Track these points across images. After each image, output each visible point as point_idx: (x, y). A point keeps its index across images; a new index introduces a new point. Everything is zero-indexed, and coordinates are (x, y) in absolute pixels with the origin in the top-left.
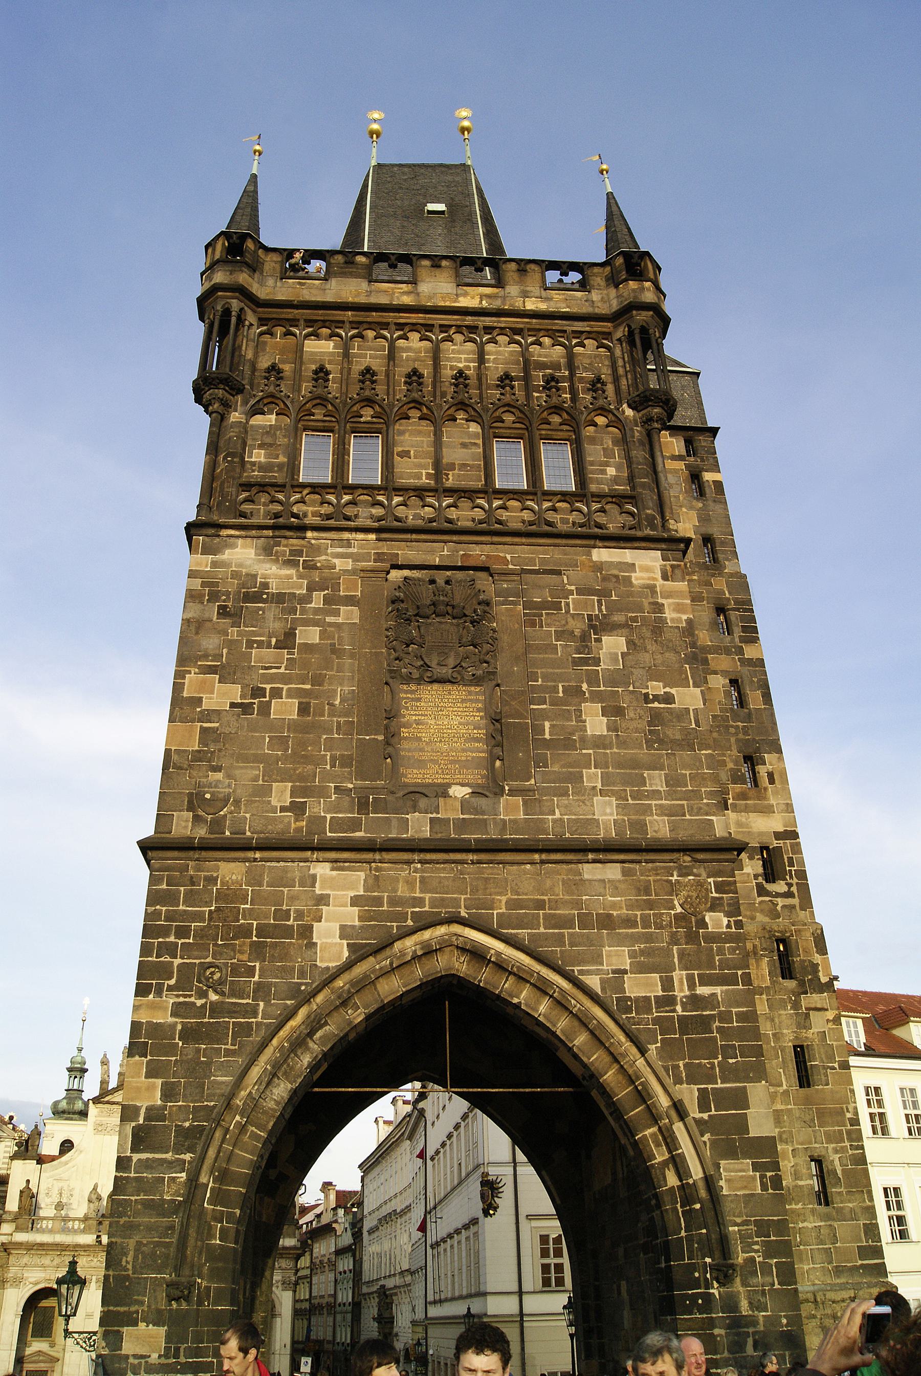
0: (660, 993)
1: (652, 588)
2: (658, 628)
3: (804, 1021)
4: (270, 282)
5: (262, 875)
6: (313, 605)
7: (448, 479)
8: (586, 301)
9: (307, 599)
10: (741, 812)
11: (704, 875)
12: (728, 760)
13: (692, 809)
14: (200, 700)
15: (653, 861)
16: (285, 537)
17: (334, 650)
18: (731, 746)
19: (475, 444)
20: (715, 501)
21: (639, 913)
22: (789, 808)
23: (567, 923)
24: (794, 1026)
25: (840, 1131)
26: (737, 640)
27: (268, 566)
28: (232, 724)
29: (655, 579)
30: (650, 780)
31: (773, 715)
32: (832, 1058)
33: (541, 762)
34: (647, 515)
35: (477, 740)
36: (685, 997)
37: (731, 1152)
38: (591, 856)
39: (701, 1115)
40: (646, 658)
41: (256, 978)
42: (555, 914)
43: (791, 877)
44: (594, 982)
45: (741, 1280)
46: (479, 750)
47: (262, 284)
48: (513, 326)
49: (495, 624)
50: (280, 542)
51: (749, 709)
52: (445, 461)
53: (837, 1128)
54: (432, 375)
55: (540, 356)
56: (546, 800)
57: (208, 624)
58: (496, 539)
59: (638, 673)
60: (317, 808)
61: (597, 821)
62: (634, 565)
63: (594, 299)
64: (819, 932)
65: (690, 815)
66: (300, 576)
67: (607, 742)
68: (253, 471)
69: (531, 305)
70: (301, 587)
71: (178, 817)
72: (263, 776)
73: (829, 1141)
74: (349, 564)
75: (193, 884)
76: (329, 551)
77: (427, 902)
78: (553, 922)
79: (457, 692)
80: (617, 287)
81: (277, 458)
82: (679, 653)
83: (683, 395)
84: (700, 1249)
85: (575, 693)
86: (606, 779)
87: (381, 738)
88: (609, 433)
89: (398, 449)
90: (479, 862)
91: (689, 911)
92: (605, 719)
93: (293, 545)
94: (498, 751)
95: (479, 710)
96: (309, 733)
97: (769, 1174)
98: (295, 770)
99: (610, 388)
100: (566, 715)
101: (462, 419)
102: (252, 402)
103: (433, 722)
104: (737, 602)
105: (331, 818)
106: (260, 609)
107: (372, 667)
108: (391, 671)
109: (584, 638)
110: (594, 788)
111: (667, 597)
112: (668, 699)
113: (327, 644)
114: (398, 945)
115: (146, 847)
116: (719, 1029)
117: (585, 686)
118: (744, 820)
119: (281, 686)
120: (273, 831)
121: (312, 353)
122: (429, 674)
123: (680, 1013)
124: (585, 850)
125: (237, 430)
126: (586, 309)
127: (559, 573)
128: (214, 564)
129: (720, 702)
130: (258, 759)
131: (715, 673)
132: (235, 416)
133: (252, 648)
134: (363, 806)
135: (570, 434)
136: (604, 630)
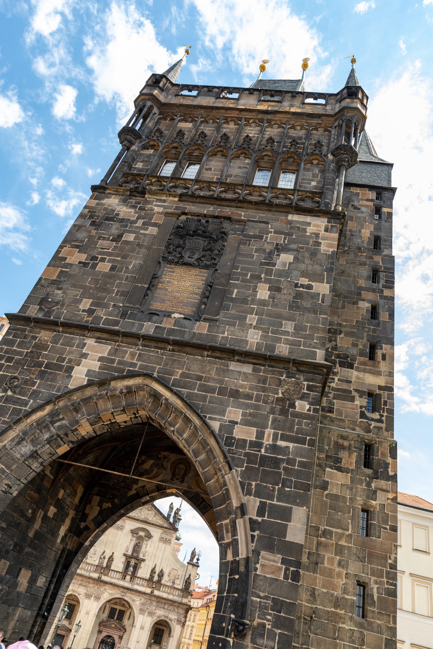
0: (254, 439)
1: (317, 235)
2: (314, 254)
3: (373, 495)
6: (136, 225)
9: (135, 222)
10: (360, 371)
12: (360, 344)
13: (306, 343)
14: (66, 258)
15: (272, 367)
17: (138, 245)
19: (246, 167)
21: (255, 393)
22: (391, 374)
23: (212, 390)
24: (365, 497)
25: (382, 571)
26: (381, 286)
28: (75, 271)
29: (321, 231)
30: (285, 325)
31: (393, 325)
32: (386, 522)
34: (325, 202)
35: (197, 294)
36: (269, 445)
37: (270, 548)
39: (257, 518)
40: (303, 267)
41: (35, 388)
42: (206, 385)
43: (383, 412)
44: (216, 425)
45: (252, 638)
46: (196, 299)
51: (380, 321)
53: (380, 567)
55: (293, 133)
57: (84, 228)
59: (295, 273)
60: (101, 313)
62: (310, 223)
64: (394, 445)
66: (136, 213)
69: (293, 110)
70: (134, 217)
73: (373, 574)
74: (161, 210)
75: (25, 338)
77: (138, 366)
78: (204, 388)
79: (194, 271)
84: (230, 607)
86: (259, 321)
87: (146, 286)
90: (173, 350)
91: (286, 397)
92: (269, 292)
94: (205, 300)
95: (202, 280)
96: (111, 279)
97: (292, 569)
98: (97, 294)
100: (248, 288)
105: (106, 318)
106: (110, 224)
108: (163, 257)
110: (251, 324)
111: (324, 240)
112: (310, 287)
114: (113, 383)
115: (10, 317)
116: (285, 469)
118: (361, 376)
120: (75, 320)
122: (182, 260)
123: (263, 453)
128: (98, 204)
129: (362, 315)
130: (81, 287)
131: (364, 300)
134: (124, 315)
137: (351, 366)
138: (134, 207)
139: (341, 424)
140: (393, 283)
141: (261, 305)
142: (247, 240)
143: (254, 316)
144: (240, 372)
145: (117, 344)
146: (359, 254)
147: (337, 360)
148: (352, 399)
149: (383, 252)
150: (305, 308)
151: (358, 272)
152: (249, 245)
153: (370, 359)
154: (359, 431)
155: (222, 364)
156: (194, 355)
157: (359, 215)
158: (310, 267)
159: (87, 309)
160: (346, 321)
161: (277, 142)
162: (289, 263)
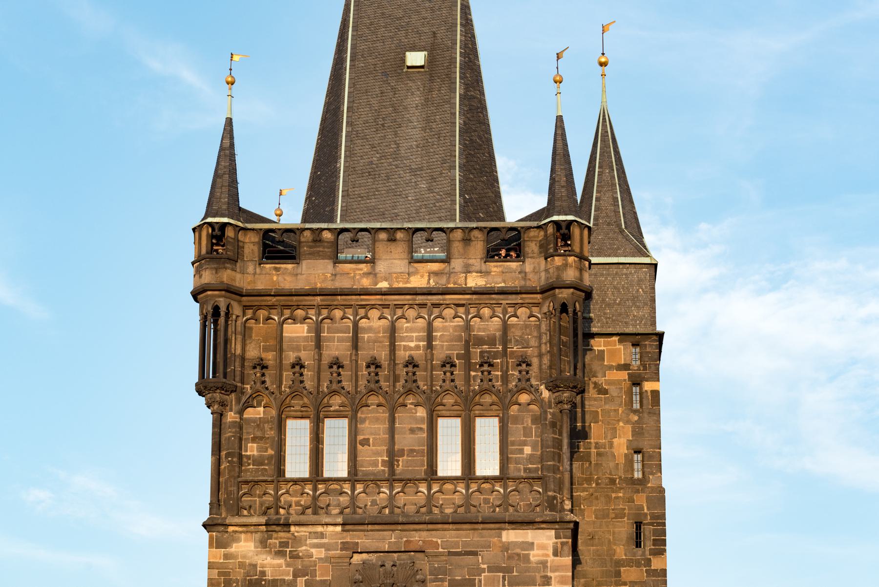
1: (544, 564)
7: (398, 466)
8: (520, 273)
19: (421, 429)
26: (647, 553)
27: (264, 557)
29: (547, 555)
34: (548, 496)
52: (396, 447)
54: (388, 357)
58: (430, 526)
62: (533, 543)
63: (527, 270)
66: (288, 565)
68: (249, 464)
70: (288, 575)
80: (546, 259)
81: (266, 451)
88: (529, 411)
89: (360, 437)
99: (535, 361)
102: (244, 399)
104: (653, 517)
121: (291, 339)
127: (475, 554)
128: (226, 557)
132: (231, 416)
138: (280, 554)
140: (664, 542)
146: (614, 495)
149: (649, 482)
157: (607, 407)
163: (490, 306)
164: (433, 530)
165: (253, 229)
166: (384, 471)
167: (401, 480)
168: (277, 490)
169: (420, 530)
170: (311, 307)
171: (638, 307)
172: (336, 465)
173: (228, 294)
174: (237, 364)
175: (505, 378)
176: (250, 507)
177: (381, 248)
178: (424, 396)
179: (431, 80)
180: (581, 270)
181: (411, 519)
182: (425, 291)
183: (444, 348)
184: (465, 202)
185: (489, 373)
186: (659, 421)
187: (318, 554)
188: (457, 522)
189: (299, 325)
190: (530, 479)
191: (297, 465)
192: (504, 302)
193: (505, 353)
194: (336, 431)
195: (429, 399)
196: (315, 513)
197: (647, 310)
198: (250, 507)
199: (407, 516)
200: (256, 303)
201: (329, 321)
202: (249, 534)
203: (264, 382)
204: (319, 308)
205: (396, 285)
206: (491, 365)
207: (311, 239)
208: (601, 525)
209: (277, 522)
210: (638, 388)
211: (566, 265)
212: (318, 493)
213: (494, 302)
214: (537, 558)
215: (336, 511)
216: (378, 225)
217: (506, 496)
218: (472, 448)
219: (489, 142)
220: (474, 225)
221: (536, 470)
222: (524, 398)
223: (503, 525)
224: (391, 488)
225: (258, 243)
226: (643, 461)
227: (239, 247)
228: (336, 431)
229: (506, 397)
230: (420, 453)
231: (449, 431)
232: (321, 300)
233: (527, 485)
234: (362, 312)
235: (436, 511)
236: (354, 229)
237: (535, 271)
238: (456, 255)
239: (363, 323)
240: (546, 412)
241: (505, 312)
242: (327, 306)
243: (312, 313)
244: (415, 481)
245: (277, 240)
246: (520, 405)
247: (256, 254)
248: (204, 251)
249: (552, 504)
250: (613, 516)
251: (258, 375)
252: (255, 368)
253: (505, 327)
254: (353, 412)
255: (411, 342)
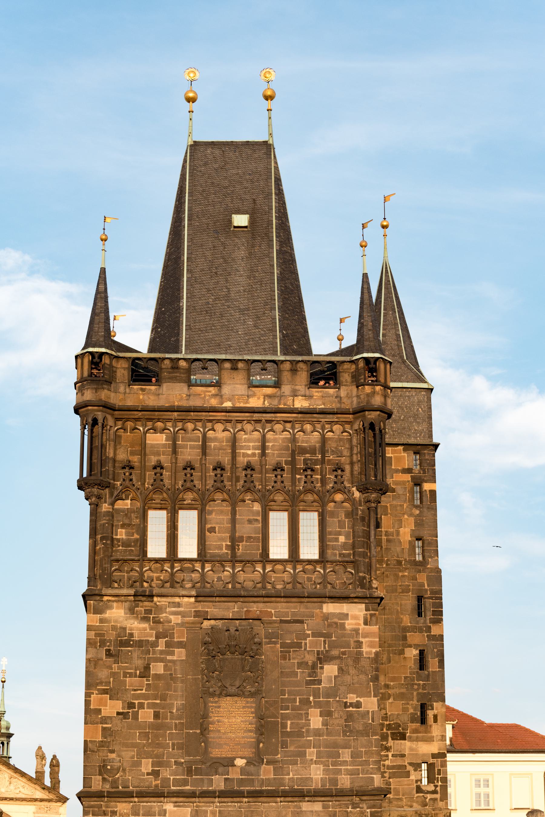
1: (357, 631)
2: (358, 657)
4: (122, 389)
5: (139, 810)
6: (159, 648)
8: (336, 397)
9: (155, 644)
10: (413, 741)
11: (365, 807)
13: (364, 770)
16: (141, 601)
17: (172, 678)
18: (413, 697)
19: (257, 520)
20: (428, 508)
26: (428, 621)
27: (132, 621)
28: (118, 725)
29: (359, 624)
30: (342, 754)
33: (284, 745)
34: (360, 577)
35: (250, 731)
38: (307, 799)
40: (348, 679)
43: (438, 782)
46: (251, 737)
47: (116, 392)
48: (285, 419)
49: (263, 657)
50: (138, 604)
51: (429, 672)
56: (286, 767)
57: (101, 662)
58: (266, 599)
59: (343, 689)
60: (166, 773)
61: (312, 778)
62: (347, 614)
63: (342, 395)
65: (362, 774)
66: (151, 629)
67: (321, 732)
68: (119, 546)
70: (152, 636)
71: (94, 779)
72: (137, 755)
76: (167, 610)
79: (240, 702)
80: (357, 387)
81: (133, 535)
82: (367, 675)
83: (418, 410)
85: (306, 702)
87: (198, 731)
88: (343, 507)
89: (208, 526)
90: (249, 802)
92: (321, 719)
93: (146, 606)
94: (260, 738)
95: (252, 713)
96: (160, 730)
98: (153, 751)
99: (347, 468)
100: (299, 717)
101: (249, 500)
103: (226, 721)
104: (432, 592)
105: (173, 779)
106: (129, 651)
107: (193, 688)
108: (204, 691)
109: (314, 666)
110: (312, 760)
112: (358, 705)
113: (167, 674)
117: (311, 698)
118: (414, 746)
119: (143, 701)
121: (153, 446)
122: (225, 692)
124: (304, 796)
125: (108, 518)
126: (333, 405)
127: (302, 622)
128: (101, 621)
129: (410, 667)
130: (134, 745)
131: (410, 646)
132: (105, 507)
133: (126, 677)
135: (318, 508)
136: (326, 661)
137: (403, 737)
138: (145, 619)
139: (399, 803)
141: (316, 736)
142: (286, 652)
143: (312, 749)
144: (312, 811)
145: (195, 804)
146: (400, 574)
147: (389, 732)
148: (408, 774)
149: (428, 564)
150: (358, 731)
151: (401, 605)
152: (290, 660)
153: (422, 723)
154: (417, 807)
155: (295, 806)
156: (269, 803)
157: (394, 503)
158: (355, 678)
159: (150, 771)
160: (393, 679)
161: (287, 463)
162: (335, 676)
163: (312, 423)
164: (268, 602)
165: (124, 358)
166: (227, 553)
167: (241, 561)
168: (141, 567)
169: (257, 602)
170: (169, 420)
171: (418, 423)
172: (188, 548)
173: (105, 409)
174: (110, 465)
175: (323, 481)
176: (120, 580)
177: (226, 375)
178: (260, 494)
179: (254, 238)
180: (385, 396)
181: (251, 593)
182: (261, 410)
183: (275, 455)
184: (284, 337)
185: (311, 476)
186: (435, 515)
187: (175, 620)
188: (288, 596)
189: (159, 434)
190: (344, 563)
191: (156, 548)
192: (323, 420)
193: (323, 461)
194: (188, 520)
195: (264, 496)
196: (172, 586)
197: (425, 425)
198: (120, 580)
199: (247, 590)
200: (126, 417)
201: (183, 432)
202: (120, 603)
203: (131, 480)
204: (176, 420)
205: (238, 405)
206: (312, 470)
207: (170, 366)
208: (390, 598)
209: (143, 594)
210: (418, 488)
211: (374, 393)
212: (175, 570)
213: (315, 420)
214: (351, 627)
215: (189, 585)
216: (223, 357)
217: (324, 576)
218: (294, 537)
219: (298, 287)
220: (300, 358)
221: (349, 555)
222: (339, 497)
223: (324, 599)
224: (233, 568)
225: (128, 368)
226: (423, 547)
227: (113, 371)
228: (188, 520)
229: (325, 496)
230: (256, 539)
231: (278, 521)
232: (178, 415)
233: (342, 567)
234: (209, 425)
235: (269, 586)
236: (205, 359)
237: (349, 396)
238: (286, 382)
239: (210, 434)
240: (357, 509)
241: (323, 428)
242: (181, 420)
243: (169, 425)
244: (252, 562)
245: (143, 366)
246: (335, 502)
247: (126, 377)
248: (86, 374)
249: (362, 583)
250: (401, 591)
251: (127, 474)
252: (124, 468)
253: (324, 440)
254: (202, 507)
255: (249, 451)
